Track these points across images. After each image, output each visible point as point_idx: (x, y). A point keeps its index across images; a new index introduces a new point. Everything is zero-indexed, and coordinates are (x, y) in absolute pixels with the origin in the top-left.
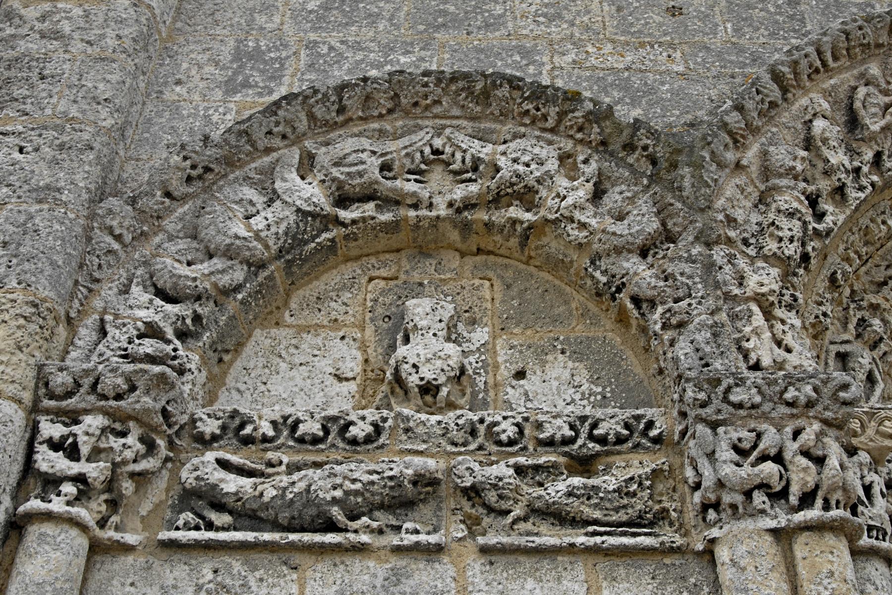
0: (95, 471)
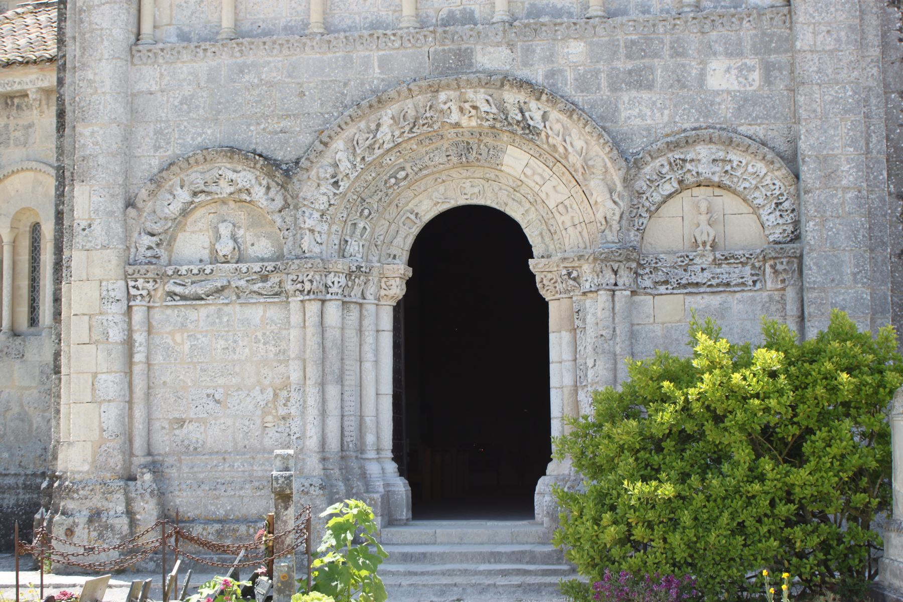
0: (144, 293)
